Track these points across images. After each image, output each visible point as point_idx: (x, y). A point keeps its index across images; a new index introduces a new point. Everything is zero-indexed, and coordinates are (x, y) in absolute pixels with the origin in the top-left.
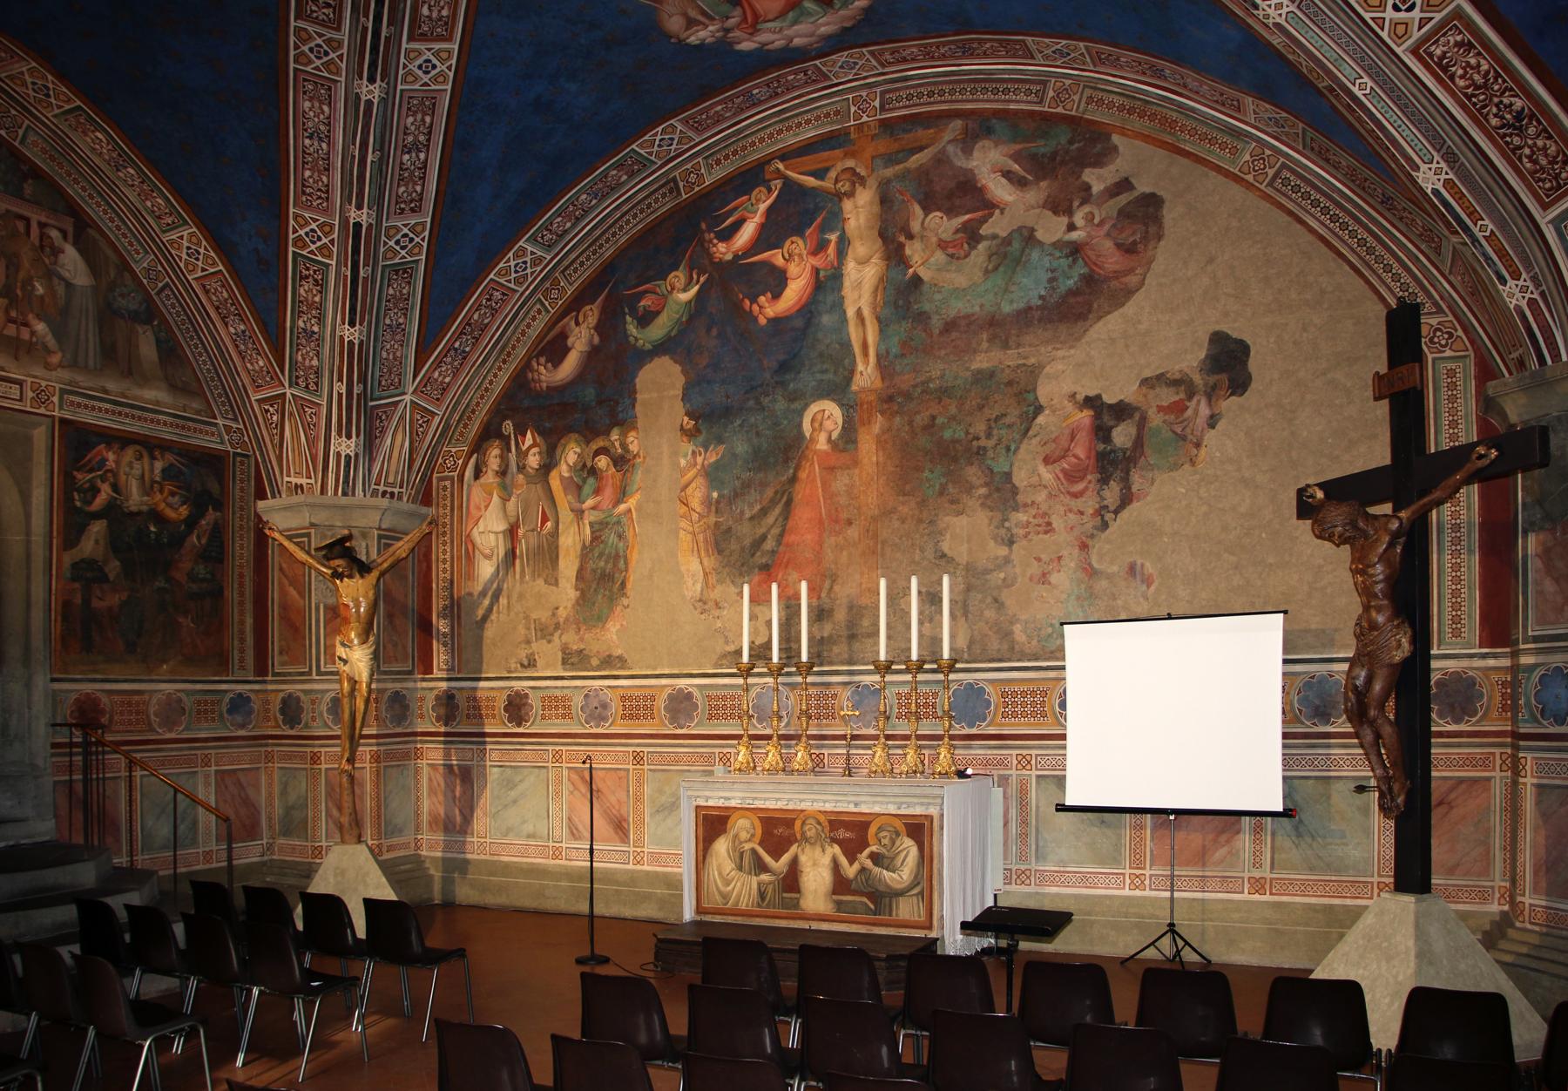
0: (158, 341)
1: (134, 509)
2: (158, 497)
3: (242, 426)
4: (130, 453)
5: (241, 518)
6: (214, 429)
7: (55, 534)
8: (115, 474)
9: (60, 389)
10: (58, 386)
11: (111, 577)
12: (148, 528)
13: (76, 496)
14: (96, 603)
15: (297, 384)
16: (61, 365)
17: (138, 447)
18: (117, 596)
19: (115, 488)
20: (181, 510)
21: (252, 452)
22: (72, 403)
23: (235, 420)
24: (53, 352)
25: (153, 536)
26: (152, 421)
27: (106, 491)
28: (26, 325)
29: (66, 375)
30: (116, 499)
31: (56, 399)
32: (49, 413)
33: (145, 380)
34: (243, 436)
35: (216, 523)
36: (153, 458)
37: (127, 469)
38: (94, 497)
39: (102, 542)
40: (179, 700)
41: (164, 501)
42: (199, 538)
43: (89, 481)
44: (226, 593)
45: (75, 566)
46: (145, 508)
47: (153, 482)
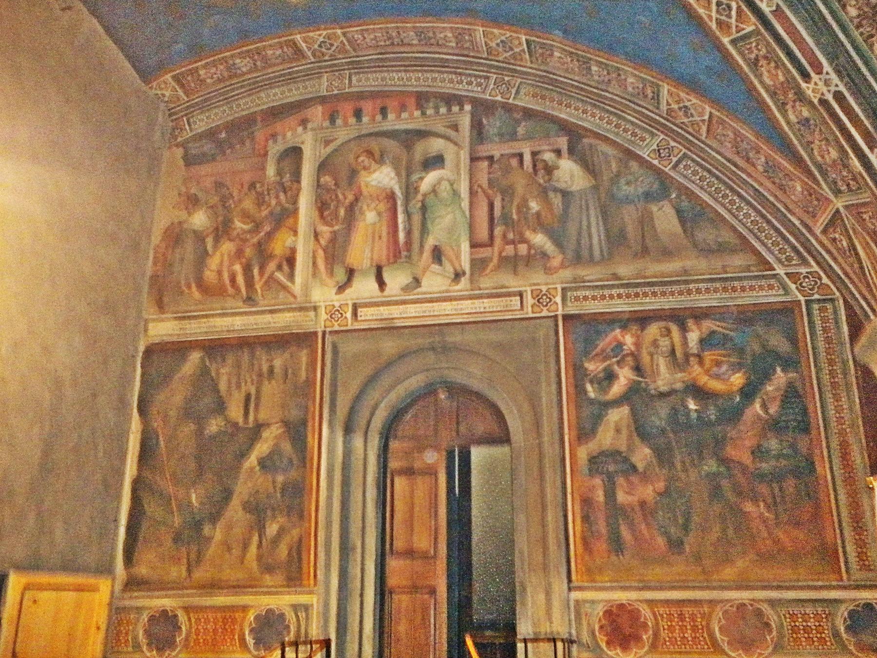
0: (679, 212)
1: (664, 389)
2: (696, 370)
3: (816, 268)
4: (653, 330)
5: (832, 373)
6: (772, 282)
7: (566, 430)
8: (635, 356)
9: (563, 289)
10: (559, 287)
11: (640, 466)
12: (686, 407)
13: (589, 387)
14: (622, 497)
15: (840, 192)
16: (563, 266)
17: (662, 324)
18: (651, 488)
19: (638, 369)
20: (733, 379)
21: (838, 294)
22: (577, 299)
23: (805, 262)
24: (553, 257)
25: (694, 415)
26: (681, 293)
27: (625, 376)
28: (524, 241)
29: (567, 274)
30: (641, 382)
31: (558, 299)
32: (552, 314)
33: (667, 253)
34: (820, 279)
35: (790, 385)
36: (684, 329)
37: (652, 349)
38: (610, 385)
39: (625, 432)
40: (759, 613)
41: (707, 372)
42: (764, 406)
43: (605, 370)
44: (819, 469)
45: (593, 460)
46: (679, 386)
47: (687, 356)
